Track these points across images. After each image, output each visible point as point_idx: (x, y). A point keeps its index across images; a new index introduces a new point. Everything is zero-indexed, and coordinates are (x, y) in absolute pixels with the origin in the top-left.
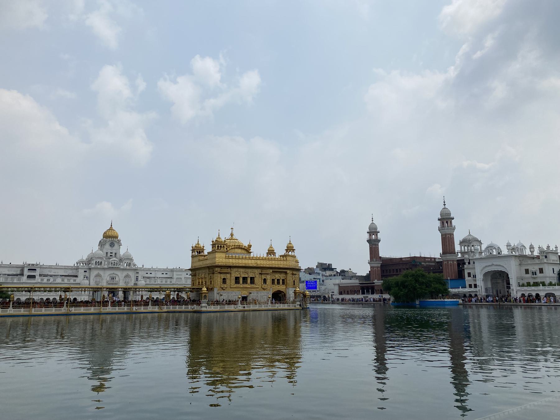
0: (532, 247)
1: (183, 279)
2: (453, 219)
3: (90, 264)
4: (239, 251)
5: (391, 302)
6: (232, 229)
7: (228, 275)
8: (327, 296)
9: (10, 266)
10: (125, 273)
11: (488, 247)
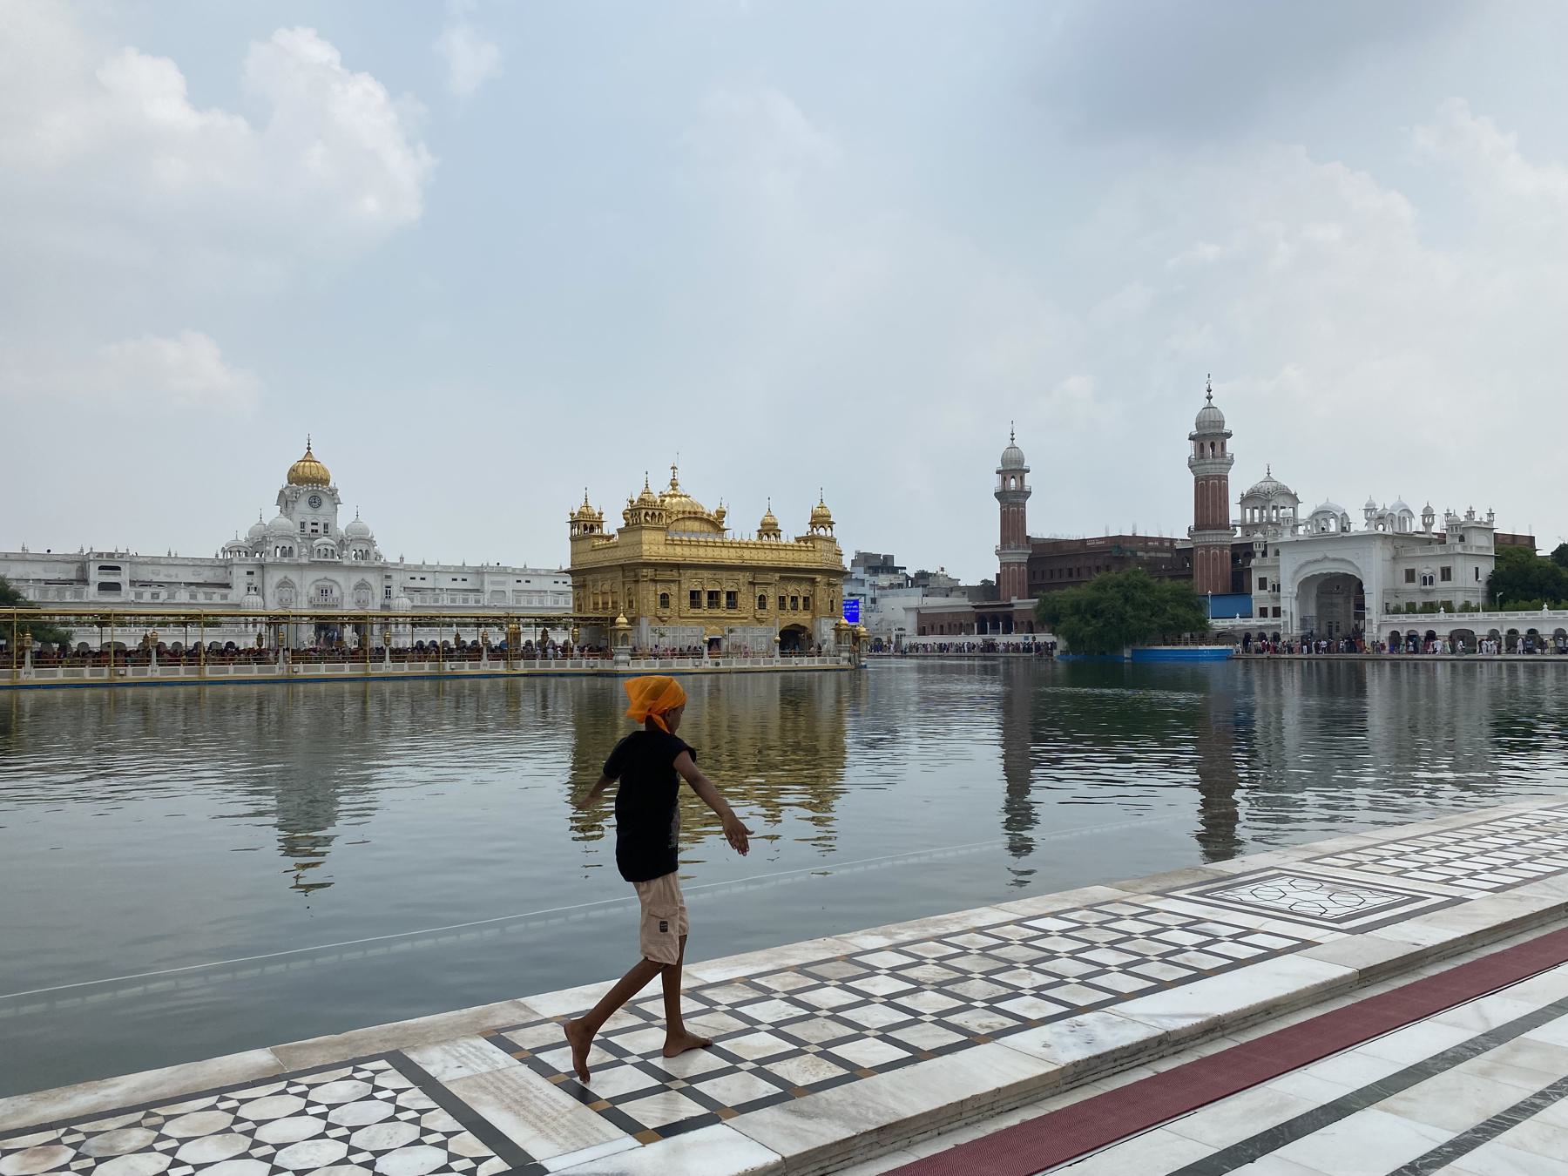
0: (1428, 514)
1: (509, 594)
2: (1229, 435)
3: (256, 551)
4: (696, 525)
5: (1056, 653)
7: (674, 587)
8: (884, 639)
9: (48, 559)
10: (356, 578)
11: (1316, 514)
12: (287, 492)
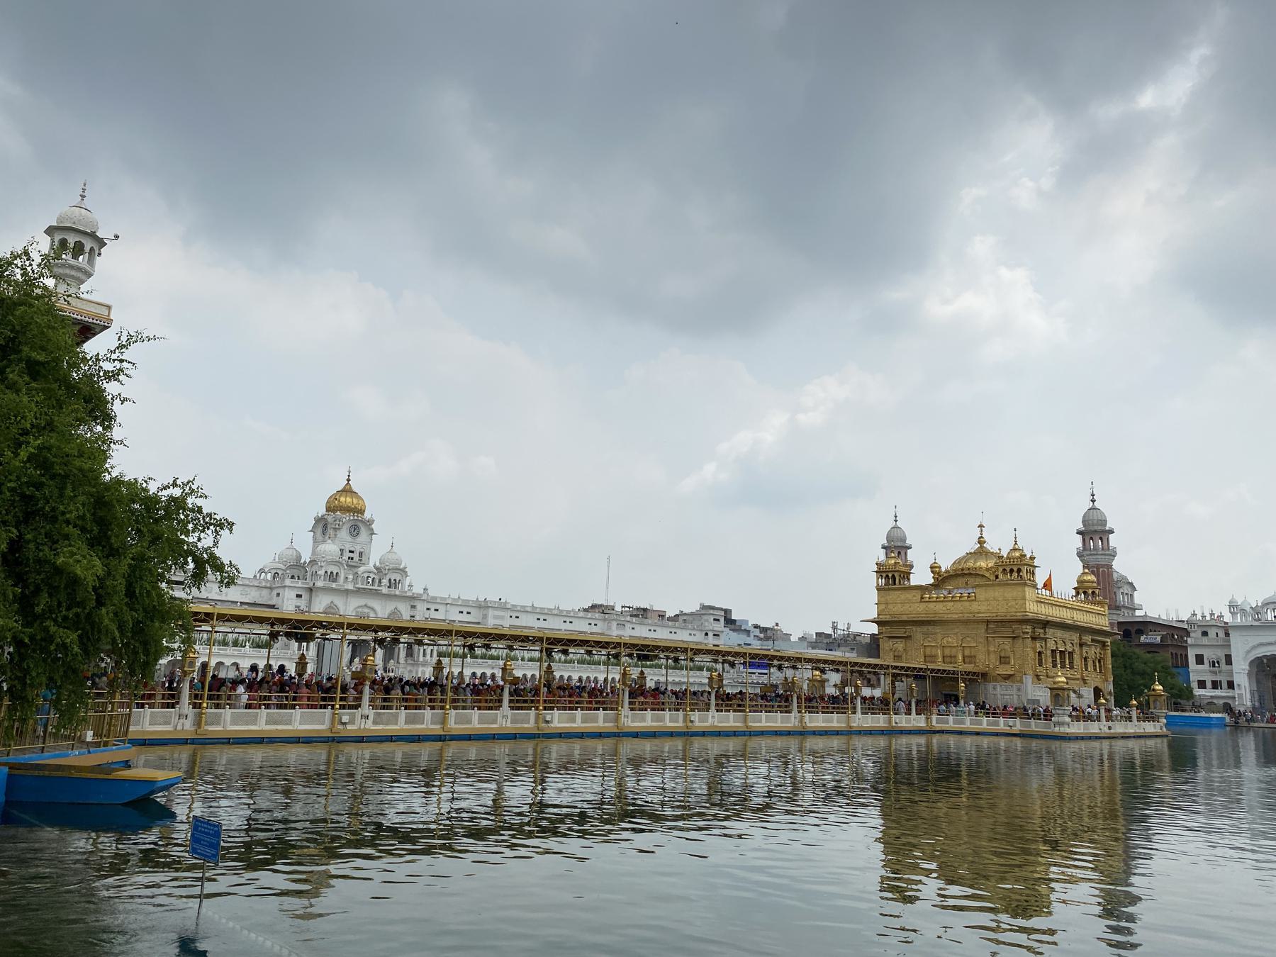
2: (1111, 532)
6: (981, 526)
12: (330, 519)
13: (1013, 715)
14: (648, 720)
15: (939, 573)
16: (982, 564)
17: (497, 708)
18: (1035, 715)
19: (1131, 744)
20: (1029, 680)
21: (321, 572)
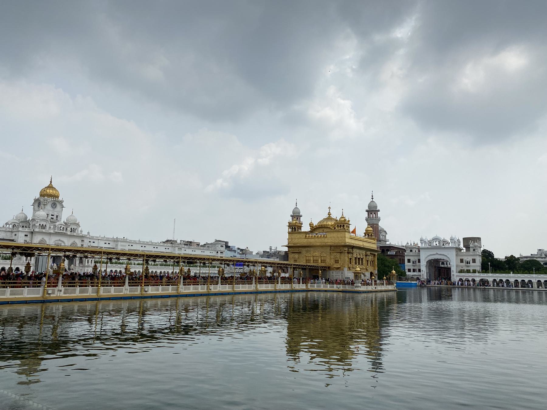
2: (379, 211)
12: (42, 200)
13: (339, 284)
14: (191, 289)
15: (313, 227)
16: (329, 223)
17: (123, 286)
18: (348, 283)
19: (383, 293)
20: (346, 269)
21: (38, 225)
